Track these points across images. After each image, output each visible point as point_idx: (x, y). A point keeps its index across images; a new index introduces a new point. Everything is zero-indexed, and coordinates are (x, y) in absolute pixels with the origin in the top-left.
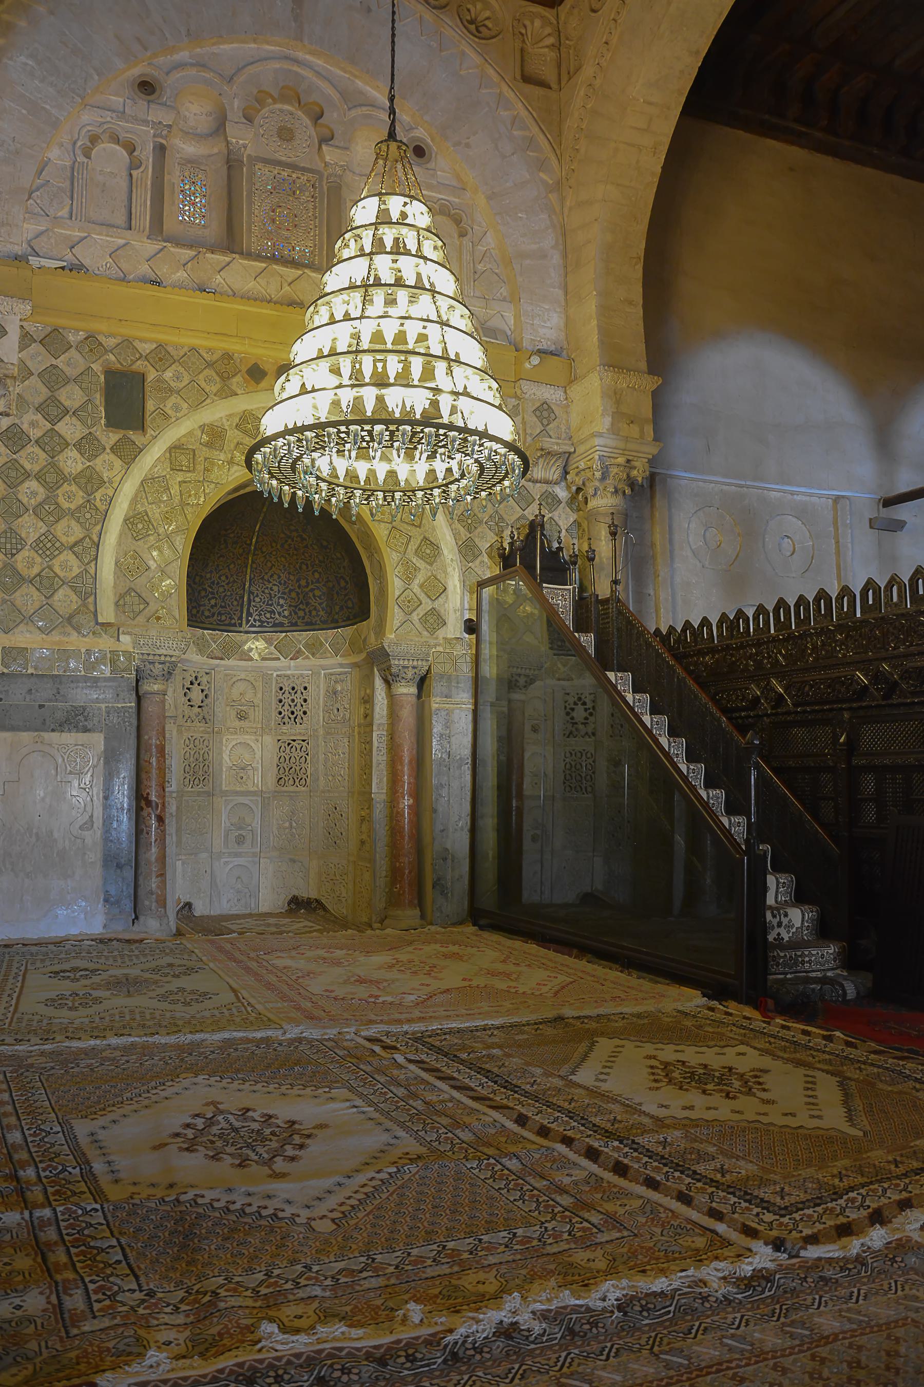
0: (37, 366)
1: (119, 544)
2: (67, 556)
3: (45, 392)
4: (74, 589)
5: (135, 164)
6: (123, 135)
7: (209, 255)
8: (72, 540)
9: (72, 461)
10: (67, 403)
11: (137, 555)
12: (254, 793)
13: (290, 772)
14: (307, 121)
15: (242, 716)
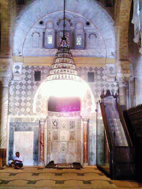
0: (24, 72)
1: (37, 100)
2: (28, 103)
3: (26, 76)
4: (30, 108)
5: (40, 36)
6: (38, 32)
7: (51, 50)
8: (29, 100)
9: (29, 87)
10: (29, 78)
11: (39, 102)
12: (66, 141)
13: (72, 138)
14: (68, 22)
15: (64, 127)
